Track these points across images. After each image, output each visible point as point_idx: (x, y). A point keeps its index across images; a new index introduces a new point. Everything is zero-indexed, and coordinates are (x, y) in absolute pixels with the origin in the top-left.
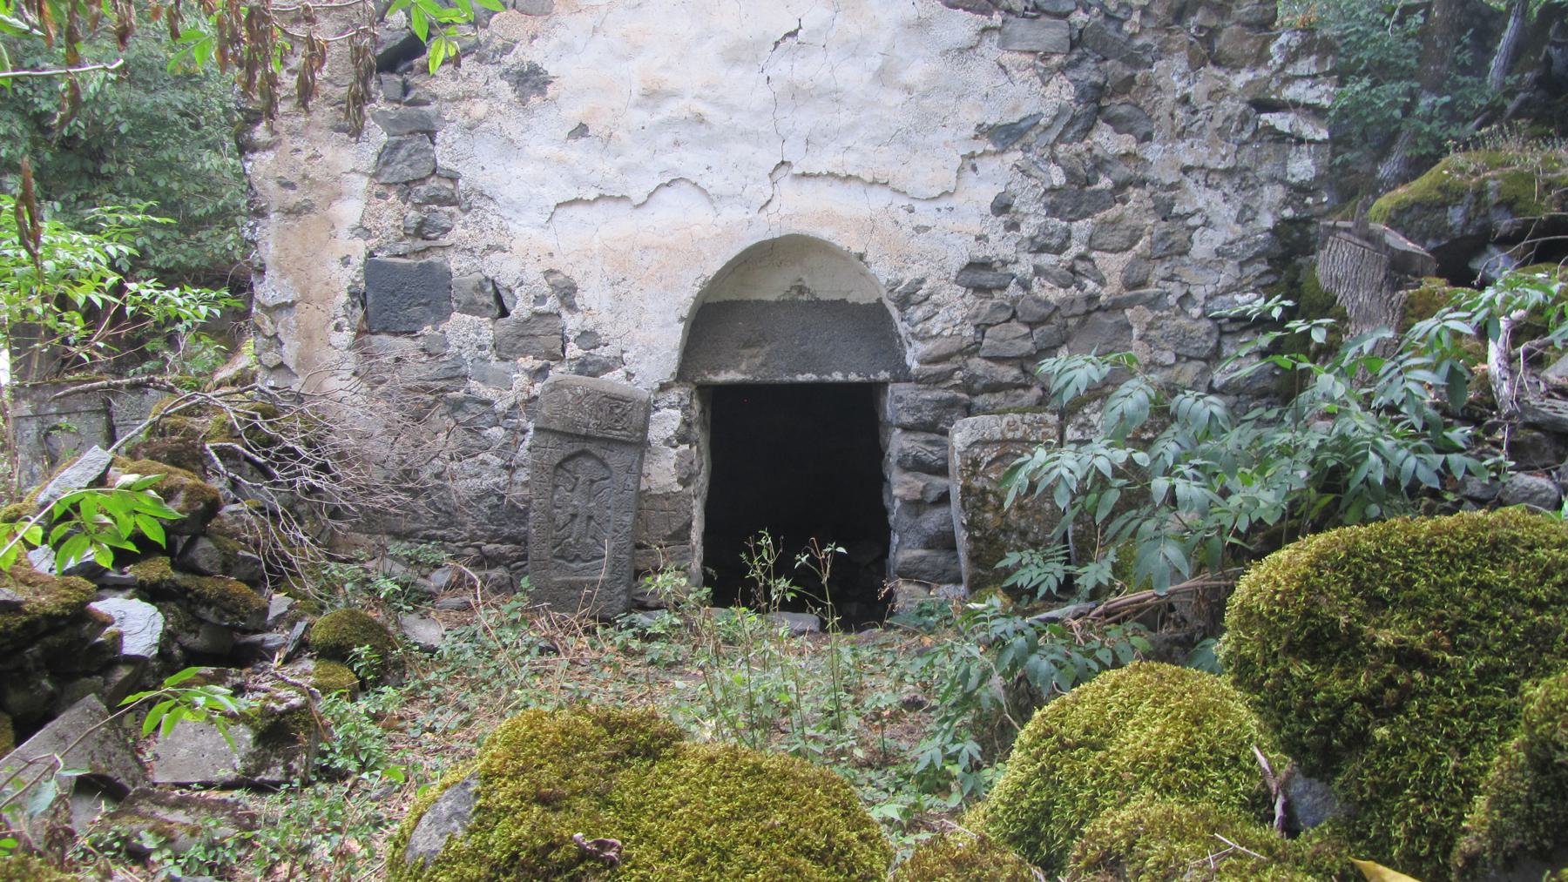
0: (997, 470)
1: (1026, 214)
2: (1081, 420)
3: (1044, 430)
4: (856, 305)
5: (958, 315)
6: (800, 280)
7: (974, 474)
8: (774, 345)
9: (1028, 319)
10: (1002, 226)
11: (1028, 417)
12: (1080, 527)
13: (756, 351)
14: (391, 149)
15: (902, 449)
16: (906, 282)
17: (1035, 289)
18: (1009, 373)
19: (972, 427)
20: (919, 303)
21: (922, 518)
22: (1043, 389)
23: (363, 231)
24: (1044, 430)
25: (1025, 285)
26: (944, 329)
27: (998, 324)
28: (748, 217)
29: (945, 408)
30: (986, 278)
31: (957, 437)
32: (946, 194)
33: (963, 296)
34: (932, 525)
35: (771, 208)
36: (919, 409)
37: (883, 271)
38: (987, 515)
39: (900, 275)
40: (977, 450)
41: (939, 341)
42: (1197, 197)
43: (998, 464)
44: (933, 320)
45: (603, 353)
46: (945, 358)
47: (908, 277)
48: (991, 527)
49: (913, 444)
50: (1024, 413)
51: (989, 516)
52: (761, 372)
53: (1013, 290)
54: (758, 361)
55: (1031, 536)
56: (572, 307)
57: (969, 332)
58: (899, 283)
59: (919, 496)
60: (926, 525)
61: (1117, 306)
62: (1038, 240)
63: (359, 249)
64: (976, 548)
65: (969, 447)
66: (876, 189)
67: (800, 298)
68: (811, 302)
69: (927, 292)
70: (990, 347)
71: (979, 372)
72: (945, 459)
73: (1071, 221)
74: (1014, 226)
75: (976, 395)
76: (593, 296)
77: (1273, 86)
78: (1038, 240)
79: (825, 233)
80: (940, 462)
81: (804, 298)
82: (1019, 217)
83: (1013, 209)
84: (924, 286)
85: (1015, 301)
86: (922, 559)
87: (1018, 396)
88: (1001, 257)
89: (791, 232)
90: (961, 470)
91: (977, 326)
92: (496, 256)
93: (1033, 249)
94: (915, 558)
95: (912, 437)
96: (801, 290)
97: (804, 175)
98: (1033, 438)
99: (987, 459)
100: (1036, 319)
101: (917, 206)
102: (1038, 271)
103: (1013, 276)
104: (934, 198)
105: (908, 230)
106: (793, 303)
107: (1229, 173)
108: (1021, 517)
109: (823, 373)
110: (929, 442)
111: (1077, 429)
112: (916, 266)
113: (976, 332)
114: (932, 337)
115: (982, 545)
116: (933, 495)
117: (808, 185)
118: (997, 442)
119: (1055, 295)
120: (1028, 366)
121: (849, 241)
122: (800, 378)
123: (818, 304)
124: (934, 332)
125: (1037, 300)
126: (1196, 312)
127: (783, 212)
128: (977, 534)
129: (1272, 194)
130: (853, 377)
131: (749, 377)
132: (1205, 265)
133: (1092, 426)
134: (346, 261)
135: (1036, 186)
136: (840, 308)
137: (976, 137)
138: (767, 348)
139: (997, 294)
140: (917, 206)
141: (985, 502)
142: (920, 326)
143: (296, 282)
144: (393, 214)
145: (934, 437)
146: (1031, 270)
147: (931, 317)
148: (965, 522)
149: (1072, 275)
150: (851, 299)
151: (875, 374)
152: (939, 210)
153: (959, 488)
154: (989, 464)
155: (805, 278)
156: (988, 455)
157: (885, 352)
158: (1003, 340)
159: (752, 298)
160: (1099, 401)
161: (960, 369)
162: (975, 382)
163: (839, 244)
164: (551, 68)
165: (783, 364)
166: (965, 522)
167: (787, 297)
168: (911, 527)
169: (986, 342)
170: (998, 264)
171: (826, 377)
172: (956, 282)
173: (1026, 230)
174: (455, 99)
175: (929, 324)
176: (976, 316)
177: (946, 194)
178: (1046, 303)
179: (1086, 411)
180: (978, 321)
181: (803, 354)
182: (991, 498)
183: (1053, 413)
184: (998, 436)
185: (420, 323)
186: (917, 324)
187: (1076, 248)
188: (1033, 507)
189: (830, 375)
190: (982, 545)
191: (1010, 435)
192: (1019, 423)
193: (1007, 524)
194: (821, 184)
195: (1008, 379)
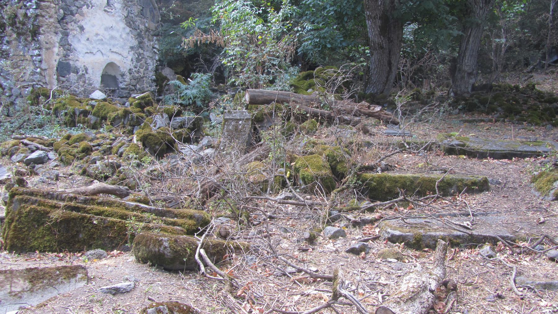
14: (62, 38)
23: (58, 55)
30: (131, 72)
42: (149, 61)
45: (91, 82)
56: (87, 73)
61: (143, 78)
63: (58, 58)
76: (90, 71)
79: (116, 62)
92: (77, 62)
96: (106, 72)
102: (135, 71)
107: (151, 57)
117: (113, 54)
119: (137, 75)
121: (118, 64)
129: (155, 61)
132: (150, 72)
134: (55, 61)
143: (48, 64)
144: (62, 52)
149: (138, 72)
164: (85, 27)
174: (72, 30)
185: (66, 75)
187: (138, 68)
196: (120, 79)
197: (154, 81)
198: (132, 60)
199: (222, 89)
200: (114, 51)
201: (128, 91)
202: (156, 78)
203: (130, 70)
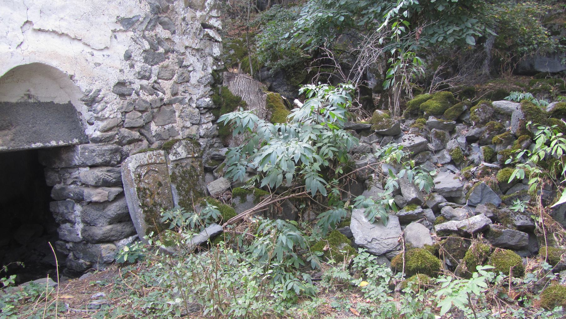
0: (147, 178)
1: (137, 61)
2: (174, 151)
3: (161, 157)
4: (58, 105)
5: (115, 107)
6: (28, 91)
7: (140, 181)
8: (18, 128)
9: (141, 109)
10: (128, 66)
11: (155, 152)
12: (182, 198)
13: (6, 132)
15: (98, 176)
16: (94, 90)
17: (141, 95)
18: (136, 134)
19: (136, 159)
20: (99, 102)
21: (106, 210)
24: (161, 157)
25: (137, 94)
26: (110, 115)
27: (130, 111)
28: (11, 50)
29: (114, 153)
30: (123, 90)
31: (130, 165)
32: (107, 48)
33: (116, 99)
34: (113, 212)
35: (22, 46)
36: (104, 155)
37: (83, 85)
39: (91, 87)
40: (139, 170)
41: (109, 120)
42: (191, 60)
43: (147, 175)
44: (105, 110)
46: (110, 129)
47: (95, 88)
48: (150, 204)
49: (102, 173)
51: (148, 200)
52: (12, 144)
53: (134, 96)
54: (8, 138)
57: (120, 116)
58: (90, 92)
59: (107, 199)
61: (170, 103)
62: (142, 73)
64: (147, 216)
65: (136, 169)
66: (76, 42)
67: (30, 101)
68: (35, 103)
69: (103, 96)
70: (129, 122)
71: (126, 135)
73: (152, 65)
74: (132, 66)
77: (207, 18)
78: (142, 73)
79: (54, 63)
81: (31, 101)
82: (134, 62)
83: (132, 58)
84: (101, 93)
85: (134, 101)
86: (111, 230)
87: (140, 145)
88: (129, 80)
89: (36, 62)
90: (135, 180)
91: (122, 113)
93: (140, 77)
94: (108, 230)
95: (101, 169)
96: (29, 96)
97: (40, 30)
98: (158, 162)
99: (143, 174)
100: (144, 109)
101: (95, 52)
102: (142, 87)
103: (133, 89)
104: (102, 50)
105: (92, 64)
106: (26, 104)
107: (198, 50)
108: (159, 198)
109: (46, 142)
110: (108, 171)
111: (174, 156)
112: (97, 83)
113: (122, 116)
114: (106, 118)
115: (149, 214)
116: (112, 197)
117: (42, 36)
118: (146, 165)
119: (149, 98)
120: (143, 131)
121: (65, 68)
122: (34, 146)
123: (40, 105)
124: (106, 116)
125: (144, 101)
126: (194, 105)
127: (30, 49)
128: (146, 209)
129: (210, 60)
130: (61, 143)
131: (5, 148)
132: (195, 86)
133: (179, 153)
135: (139, 48)
136: (50, 106)
137: (116, 22)
138: (14, 130)
139: (128, 98)
140: (95, 52)
141: (146, 193)
142: (100, 113)
145: (110, 168)
146: (139, 87)
147: (104, 109)
149: (154, 89)
150: (56, 101)
151: (71, 141)
152: (104, 56)
153: (136, 189)
154: (145, 175)
155: (32, 90)
156: (143, 171)
157: (75, 129)
158: (133, 119)
159: (3, 101)
161: (117, 134)
162: (124, 139)
163: (61, 69)
165: (24, 138)
167: (23, 100)
168: (101, 215)
169: (127, 120)
170: (128, 83)
171: (48, 145)
172: (113, 92)
173: (137, 69)
175: (103, 112)
176: (122, 108)
177: (107, 48)
178: (146, 102)
179: (175, 147)
180: (123, 110)
181: (35, 132)
182: (148, 191)
184: (146, 162)
186: (99, 112)
187: (154, 78)
188: (162, 193)
189: (49, 143)
190: (149, 214)
191: (150, 161)
193: (155, 202)
194: (48, 37)
195: (137, 137)
196: (85, 113)
197: (208, 109)
198: (128, 57)
199: (382, 127)
200: (49, 26)
201: (114, 146)
202: (214, 102)
203: (121, 84)
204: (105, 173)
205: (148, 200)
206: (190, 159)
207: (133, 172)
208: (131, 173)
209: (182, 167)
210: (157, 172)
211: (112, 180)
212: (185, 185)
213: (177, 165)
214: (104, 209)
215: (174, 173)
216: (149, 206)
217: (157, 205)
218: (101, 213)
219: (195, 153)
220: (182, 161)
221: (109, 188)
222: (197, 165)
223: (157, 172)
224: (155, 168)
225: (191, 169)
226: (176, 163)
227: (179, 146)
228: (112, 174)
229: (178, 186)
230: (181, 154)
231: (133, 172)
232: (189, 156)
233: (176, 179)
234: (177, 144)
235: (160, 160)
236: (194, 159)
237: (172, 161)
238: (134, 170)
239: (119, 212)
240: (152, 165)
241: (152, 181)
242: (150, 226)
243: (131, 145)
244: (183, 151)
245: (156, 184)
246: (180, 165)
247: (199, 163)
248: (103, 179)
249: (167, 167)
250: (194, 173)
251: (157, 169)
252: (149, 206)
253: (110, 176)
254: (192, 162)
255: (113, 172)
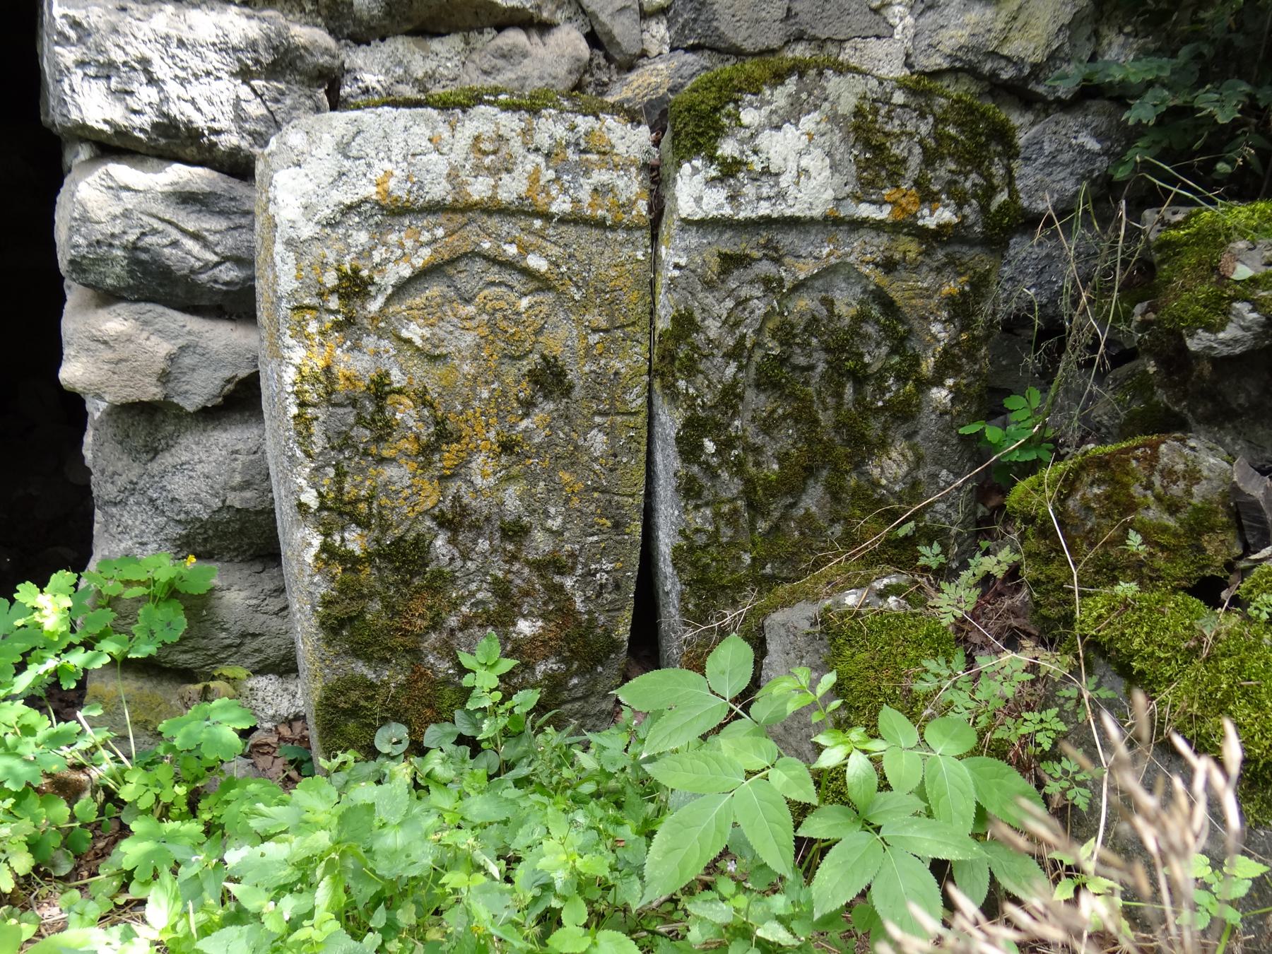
0: (430, 314)
3: (600, 176)
11: (550, 129)
12: (701, 518)
21: (167, 459)
22: (593, 39)
24: (600, 176)
34: (200, 485)
38: (390, 472)
43: (435, 290)
50: (534, 111)
51: (398, 474)
55: (540, 543)
59: (151, 391)
60: (179, 486)
65: (331, 224)
72: (244, 261)
75: (360, 39)
80: (229, 273)
98: (561, 205)
108: (509, 479)
118: (434, 208)
128: (355, 541)
148: (310, 498)
154: (402, 288)
160: (791, 84)
166: (310, 498)
168: (133, 488)
182: (405, 413)
183: (633, 117)
184: (438, 191)
188: (550, 444)
191: (479, 189)
192: (516, 145)
204: (159, 208)
205: (398, 474)
206: (867, 235)
207: (290, 243)
208: (279, 248)
209: (772, 285)
210: (540, 283)
211: (207, 267)
212: (768, 426)
213: (731, 262)
214: (155, 452)
215: (685, 324)
216: (385, 527)
217: (476, 528)
218: (136, 470)
219: (929, 198)
220: (787, 240)
221: (194, 324)
222: (927, 294)
223: (540, 283)
224: (525, 250)
225: (861, 318)
226: (728, 243)
227: (794, 113)
228: (219, 224)
229: (690, 423)
230: (785, 181)
231: (290, 243)
232: (866, 211)
233: (691, 370)
234: (780, 96)
235: (585, 195)
236: (910, 248)
237: (687, 223)
238: (307, 231)
239: (235, 500)
240: (493, 223)
241: (469, 339)
242: (362, 669)
243: (436, 45)
244: (816, 162)
245: (511, 372)
246: (766, 268)
247: (951, 287)
248: (134, 248)
249: (655, 262)
250: (875, 356)
251: (536, 262)
252: (385, 527)
253: (196, 236)
254: (889, 266)
255: (222, 213)
